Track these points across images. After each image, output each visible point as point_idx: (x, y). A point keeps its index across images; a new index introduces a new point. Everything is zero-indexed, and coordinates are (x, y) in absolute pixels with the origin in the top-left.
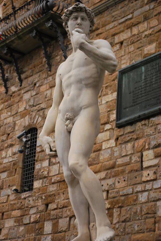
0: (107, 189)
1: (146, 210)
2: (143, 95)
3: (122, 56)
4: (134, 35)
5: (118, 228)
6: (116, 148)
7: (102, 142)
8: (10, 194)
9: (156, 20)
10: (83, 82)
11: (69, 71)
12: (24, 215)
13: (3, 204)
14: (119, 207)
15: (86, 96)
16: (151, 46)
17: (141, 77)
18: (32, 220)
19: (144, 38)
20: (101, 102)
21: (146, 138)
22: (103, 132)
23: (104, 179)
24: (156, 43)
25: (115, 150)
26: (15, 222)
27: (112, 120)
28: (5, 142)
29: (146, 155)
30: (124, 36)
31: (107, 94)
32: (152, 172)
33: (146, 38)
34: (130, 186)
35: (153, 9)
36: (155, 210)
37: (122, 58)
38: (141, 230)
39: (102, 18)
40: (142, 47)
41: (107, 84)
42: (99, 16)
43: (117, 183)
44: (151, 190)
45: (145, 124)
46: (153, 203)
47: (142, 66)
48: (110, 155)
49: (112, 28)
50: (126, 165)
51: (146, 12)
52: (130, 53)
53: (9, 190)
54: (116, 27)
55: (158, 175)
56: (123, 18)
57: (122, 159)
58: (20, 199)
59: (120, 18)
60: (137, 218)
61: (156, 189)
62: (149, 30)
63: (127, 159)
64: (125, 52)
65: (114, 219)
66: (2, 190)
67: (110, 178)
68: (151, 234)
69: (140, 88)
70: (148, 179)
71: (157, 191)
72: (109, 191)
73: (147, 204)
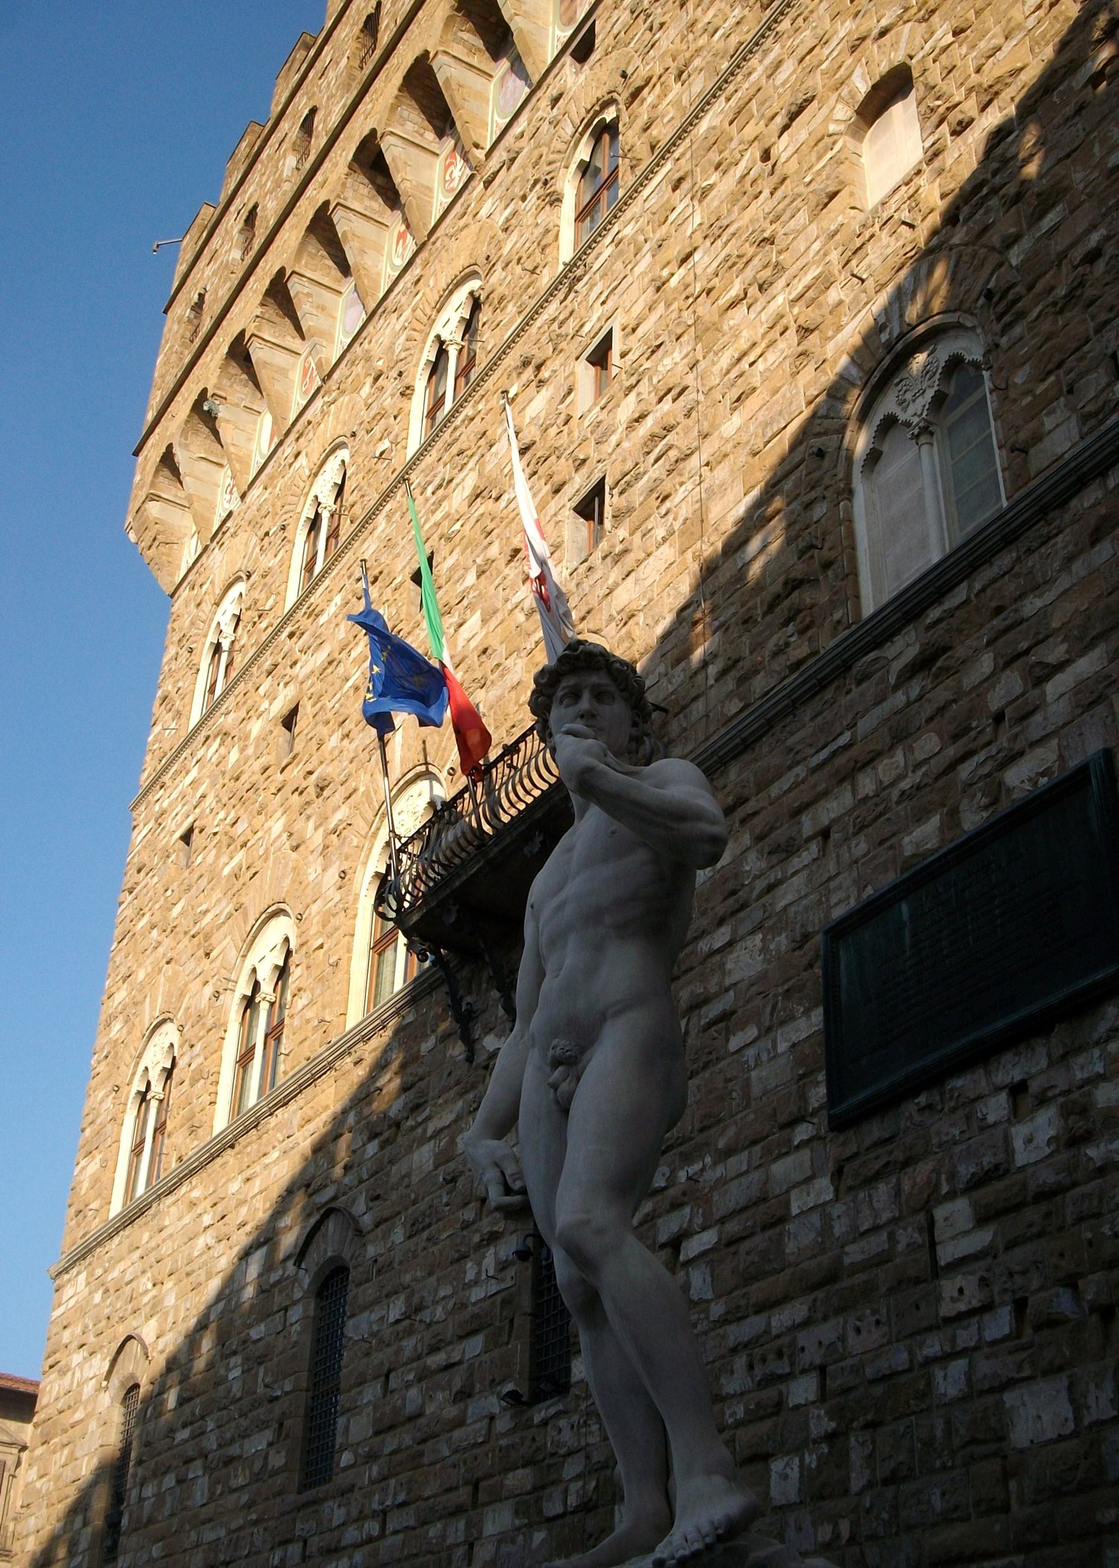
0: (818, 1361)
3: (830, 879)
4: (866, 799)
5: (871, 1507)
6: (838, 1205)
7: (788, 1191)
8: (496, 1410)
10: (608, 920)
11: (561, 888)
12: (543, 1487)
13: (475, 1451)
14: (867, 1426)
15: (622, 968)
18: (572, 1501)
19: (898, 803)
20: (775, 1047)
21: (939, 1156)
22: (787, 1154)
23: (807, 1323)
25: (835, 1216)
26: (517, 1513)
27: (816, 1105)
28: (475, 1227)
29: (946, 1219)
30: (830, 810)
31: (792, 1018)
32: (974, 1280)
34: (898, 1341)
35: (920, 698)
37: (832, 884)
38: (956, 1508)
39: (755, 760)
40: (894, 834)
41: (791, 983)
42: (747, 757)
43: (851, 1334)
44: (976, 1348)
45: (930, 1107)
46: (989, 1400)
48: (819, 1234)
49: (790, 790)
50: (878, 1264)
52: (856, 862)
53: (494, 1399)
54: (803, 782)
55: (996, 1290)
56: (823, 748)
57: (863, 1243)
58: (529, 1428)
59: (813, 751)
60: (938, 1464)
61: (994, 1343)
63: (879, 1242)
64: (838, 863)
65: (853, 1475)
66: (469, 1401)
67: (825, 1319)
70: (962, 1307)
72: (829, 1369)
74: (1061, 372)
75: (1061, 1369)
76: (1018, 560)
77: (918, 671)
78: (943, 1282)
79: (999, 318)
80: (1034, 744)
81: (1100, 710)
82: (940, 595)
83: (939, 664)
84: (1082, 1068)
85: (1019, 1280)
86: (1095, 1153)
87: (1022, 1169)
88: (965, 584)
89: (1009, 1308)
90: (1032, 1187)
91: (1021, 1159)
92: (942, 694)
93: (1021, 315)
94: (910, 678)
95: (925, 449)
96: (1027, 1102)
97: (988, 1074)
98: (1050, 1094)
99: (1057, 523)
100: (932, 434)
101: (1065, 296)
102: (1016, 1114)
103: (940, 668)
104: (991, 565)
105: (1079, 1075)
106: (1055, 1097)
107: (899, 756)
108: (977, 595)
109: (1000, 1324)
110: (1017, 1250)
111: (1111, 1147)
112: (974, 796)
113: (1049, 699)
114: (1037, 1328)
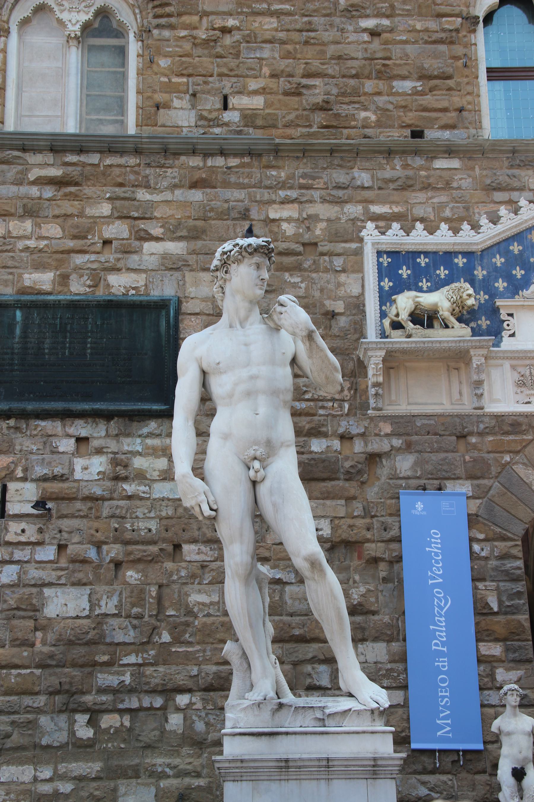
1: (15, 602)
2: (16, 368)
9: (58, 226)
16: (40, 275)
17: (12, 331)
21: (18, 456)
24: (55, 274)
29: (17, 490)
33: (28, 254)
36: (37, 604)
40: (15, 267)
44: (26, 562)
46: (34, 590)
47: (17, 307)
51: (28, 198)
55: (47, 536)
62: (37, 239)
68: (25, 651)
69: (9, 351)
70: (23, 539)
71: (45, 567)
73: (16, 590)
74: (191, 79)
75: (85, 584)
76: (139, 165)
77: (51, 184)
78: (10, 523)
79: (156, 17)
80: (129, 270)
81: (177, 275)
82: (81, 151)
83: (73, 189)
84: (128, 445)
85: (65, 535)
86: (129, 488)
87: (78, 481)
88: (98, 155)
89: (55, 547)
90: (86, 492)
91: (78, 475)
92: (68, 207)
93: (171, 27)
94: (46, 184)
95: (74, 50)
96: (83, 448)
97: (64, 426)
98: (105, 450)
99: (171, 162)
100: (79, 42)
101: (204, 40)
102: (77, 453)
103: (71, 193)
104: (121, 156)
105: (126, 448)
106: (107, 452)
107: (28, 225)
108: (104, 166)
109: (48, 553)
110: (65, 519)
111: (139, 488)
112: (83, 276)
113: (144, 251)
114: (73, 561)
